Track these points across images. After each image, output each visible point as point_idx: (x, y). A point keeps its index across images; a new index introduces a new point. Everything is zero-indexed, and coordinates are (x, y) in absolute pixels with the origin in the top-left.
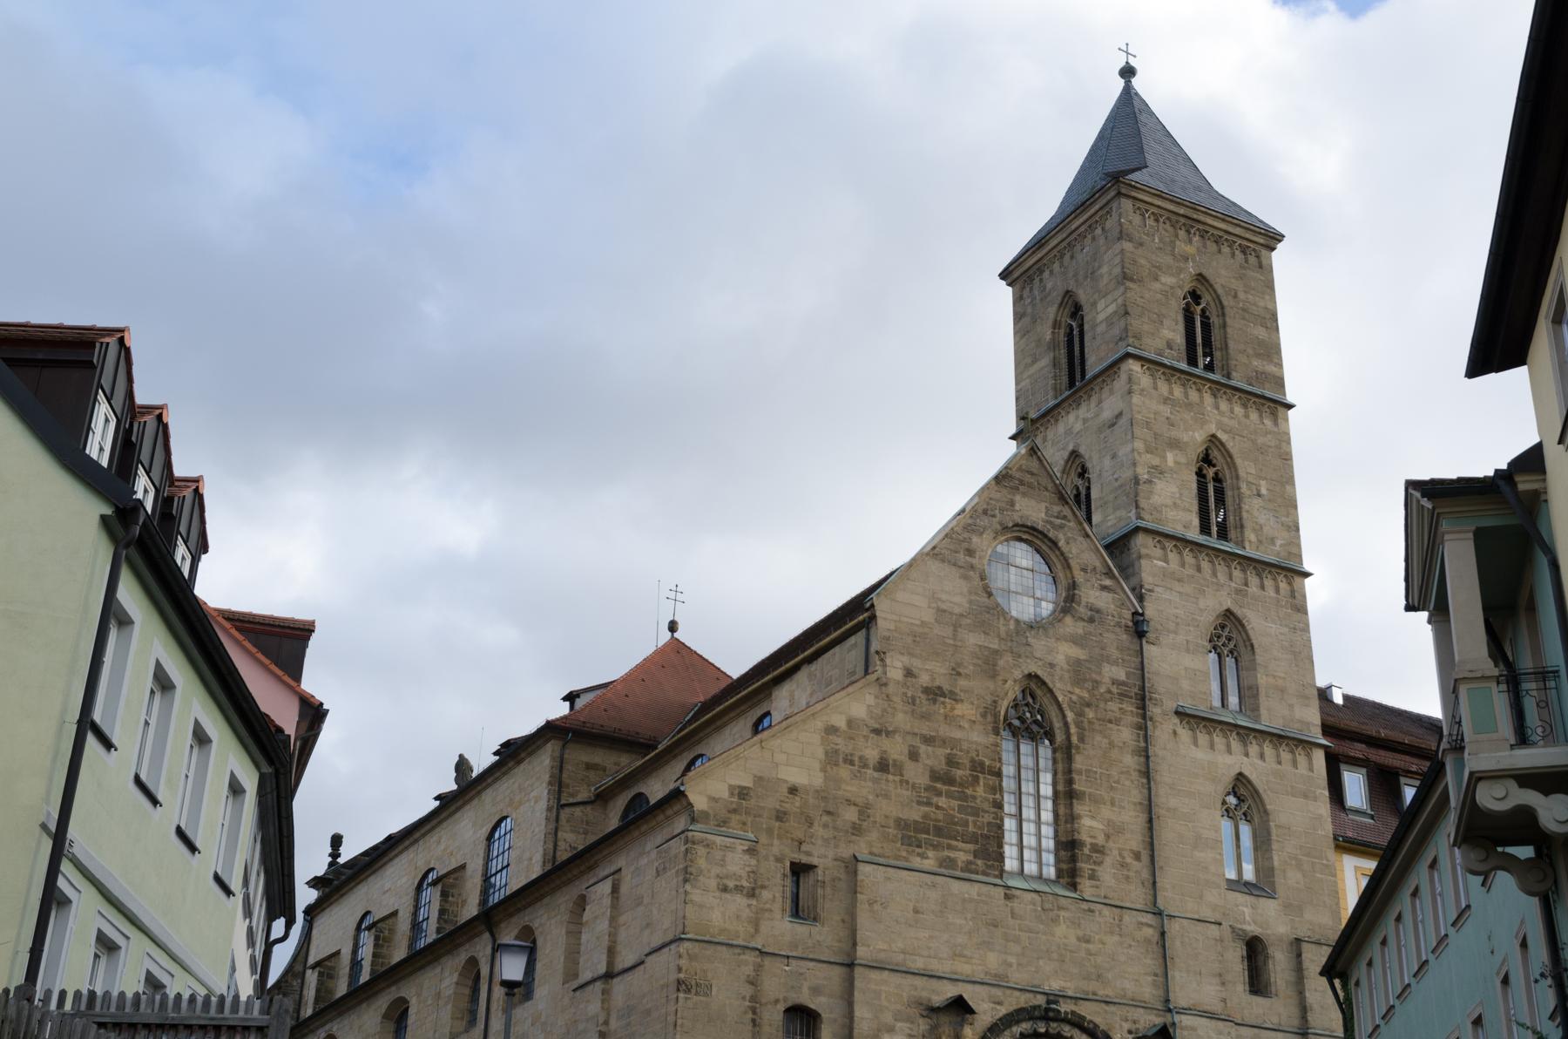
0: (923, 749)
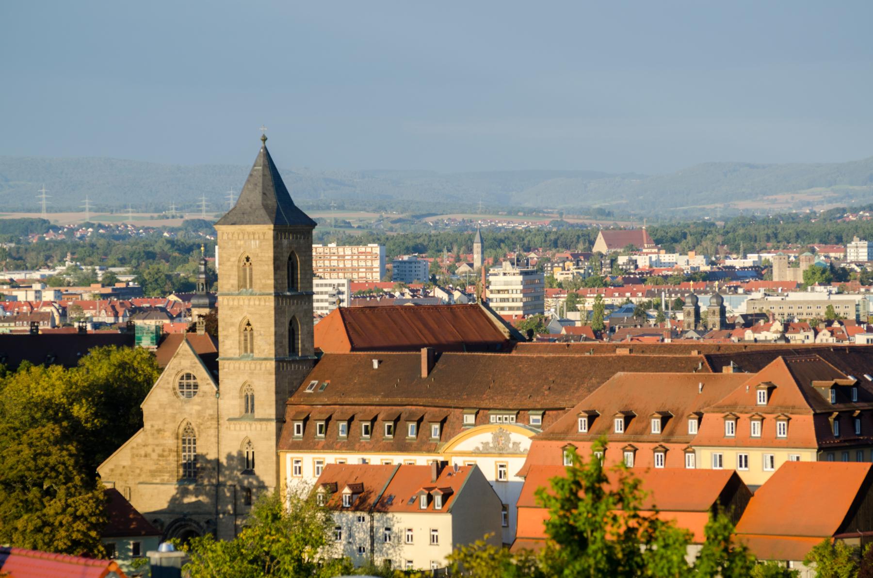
0: (156, 448)
